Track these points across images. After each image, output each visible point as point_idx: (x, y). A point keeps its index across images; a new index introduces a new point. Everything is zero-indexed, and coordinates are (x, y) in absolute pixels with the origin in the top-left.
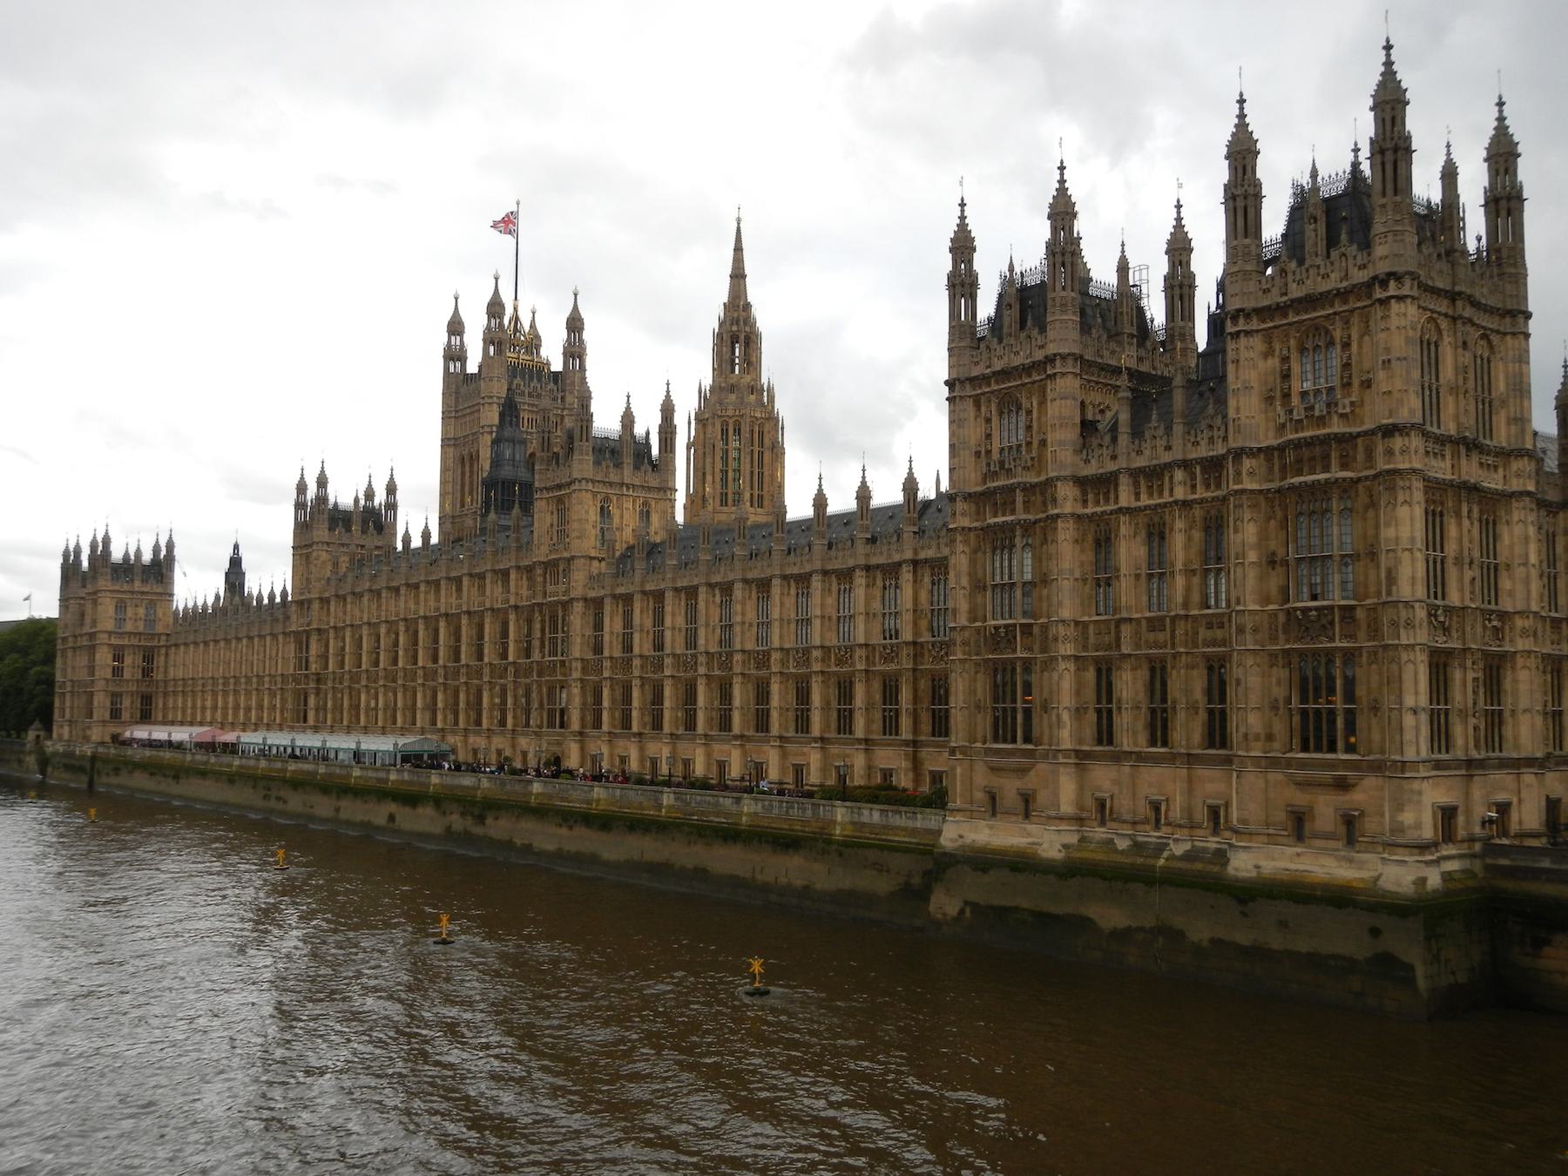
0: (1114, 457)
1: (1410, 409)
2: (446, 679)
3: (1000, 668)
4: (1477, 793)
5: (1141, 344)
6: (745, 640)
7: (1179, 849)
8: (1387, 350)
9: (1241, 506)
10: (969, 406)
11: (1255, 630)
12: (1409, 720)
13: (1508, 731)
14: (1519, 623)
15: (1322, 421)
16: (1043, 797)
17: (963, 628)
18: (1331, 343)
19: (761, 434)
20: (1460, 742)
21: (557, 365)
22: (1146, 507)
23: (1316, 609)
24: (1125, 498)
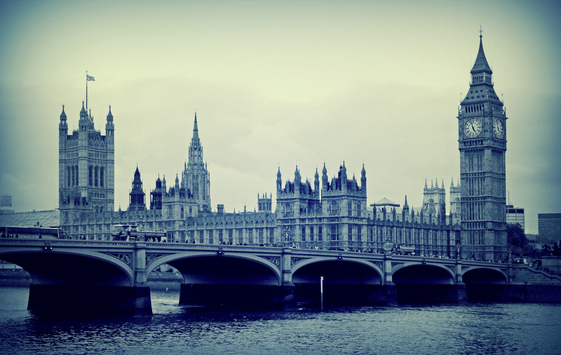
0: (305, 216)
5: (310, 194)
11: (326, 244)
14: (364, 243)
15: (335, 215)
17: (280, 242)
18: (336, 203)
19: (204, 178)
21: (103, 133)
24: (307, 222)
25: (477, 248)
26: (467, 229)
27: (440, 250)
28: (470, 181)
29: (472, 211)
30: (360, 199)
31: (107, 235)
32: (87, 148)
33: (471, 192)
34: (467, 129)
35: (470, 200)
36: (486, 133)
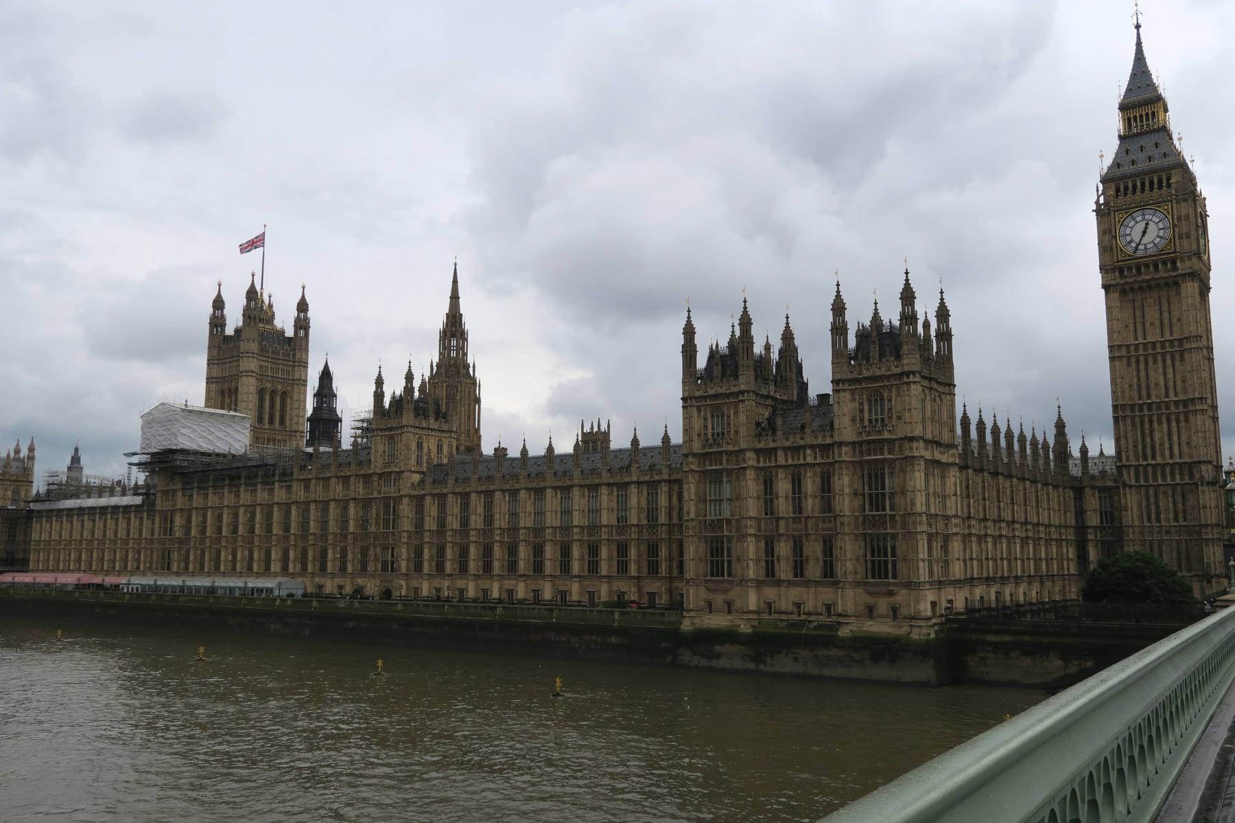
0: (774, 441)
1: (918, 432)
2: (295, 542)
3: (714, 540)
4: (943, 597)
6: (526, 521)
7: (812, 626)
8: (910, 404)
9: (841, 468)
10: (695, 409)
11: (849, 524)
12: (921, 564)
13: (951, 568)
15: (879, 432)
16: (738, 604)
17: (693, 520)
18: (882, 399)
20: (936, 573)
21: (290, 333)
22: (792, 465)
23: (879, 515)
24: (781, 460)
25: (1168, 532)
26: (1133, 483)
27: (1064, 537)
28: (1138, 362)
29: (1148, 439)
30: (941, 389)
31: (249, 510)
32: (255, 356)
33: (1144, 392)
34: (1126, 235)
35: (1141, 410)
36: (1185, 242)
